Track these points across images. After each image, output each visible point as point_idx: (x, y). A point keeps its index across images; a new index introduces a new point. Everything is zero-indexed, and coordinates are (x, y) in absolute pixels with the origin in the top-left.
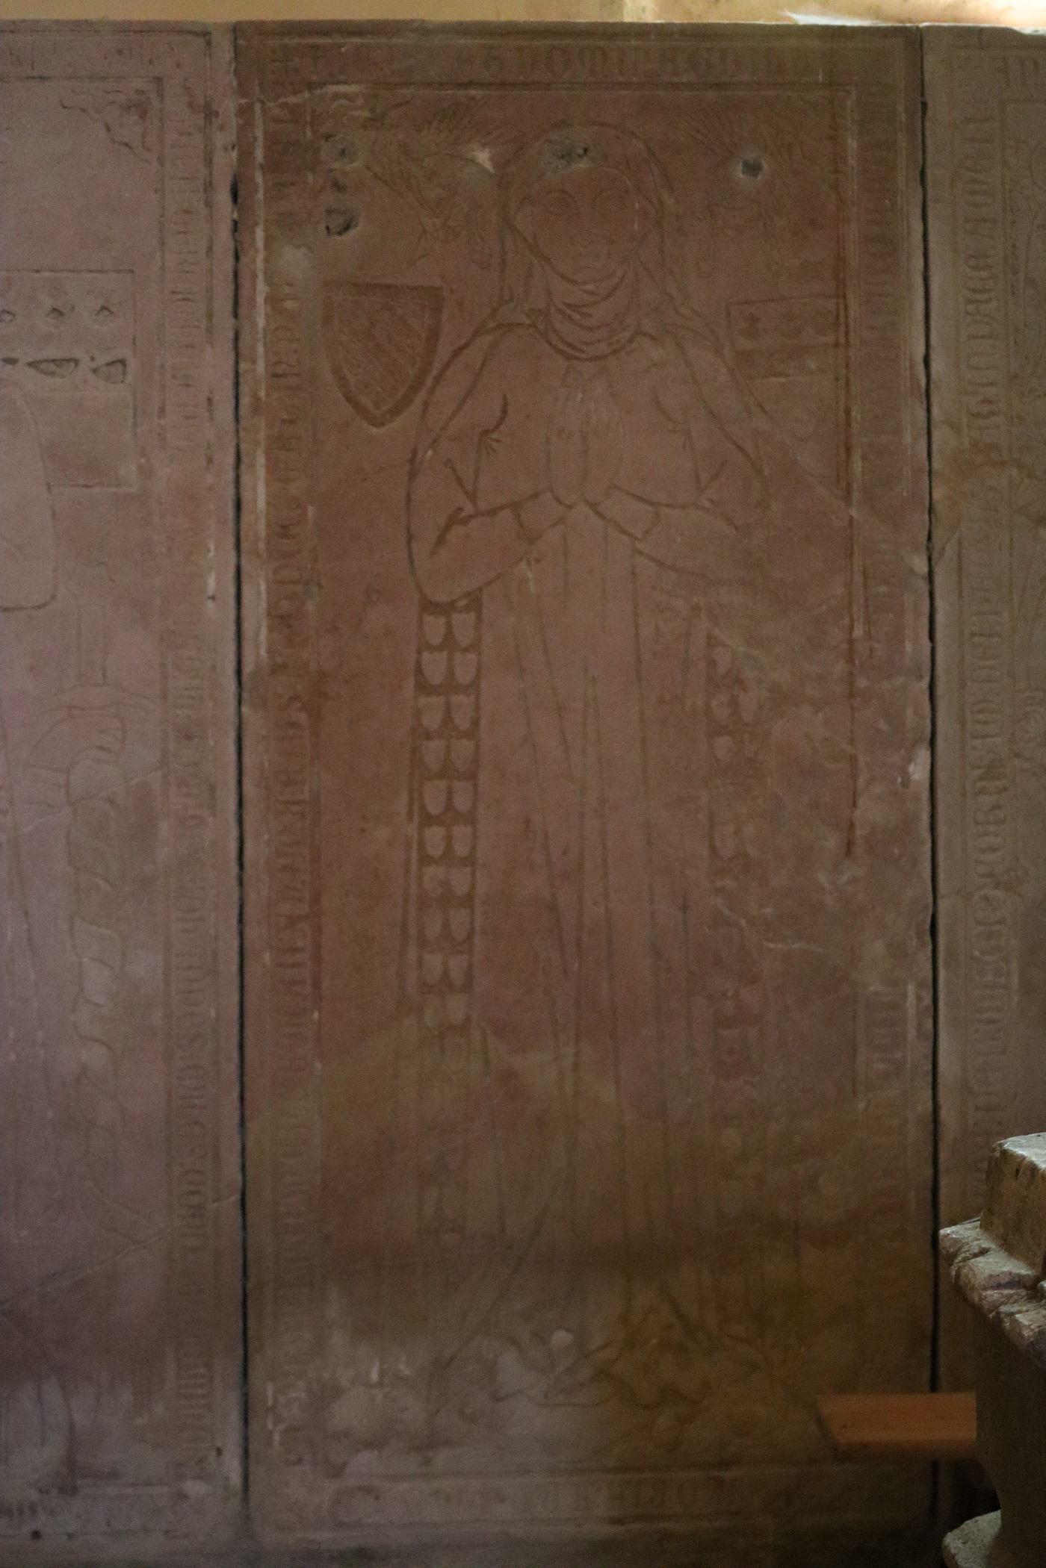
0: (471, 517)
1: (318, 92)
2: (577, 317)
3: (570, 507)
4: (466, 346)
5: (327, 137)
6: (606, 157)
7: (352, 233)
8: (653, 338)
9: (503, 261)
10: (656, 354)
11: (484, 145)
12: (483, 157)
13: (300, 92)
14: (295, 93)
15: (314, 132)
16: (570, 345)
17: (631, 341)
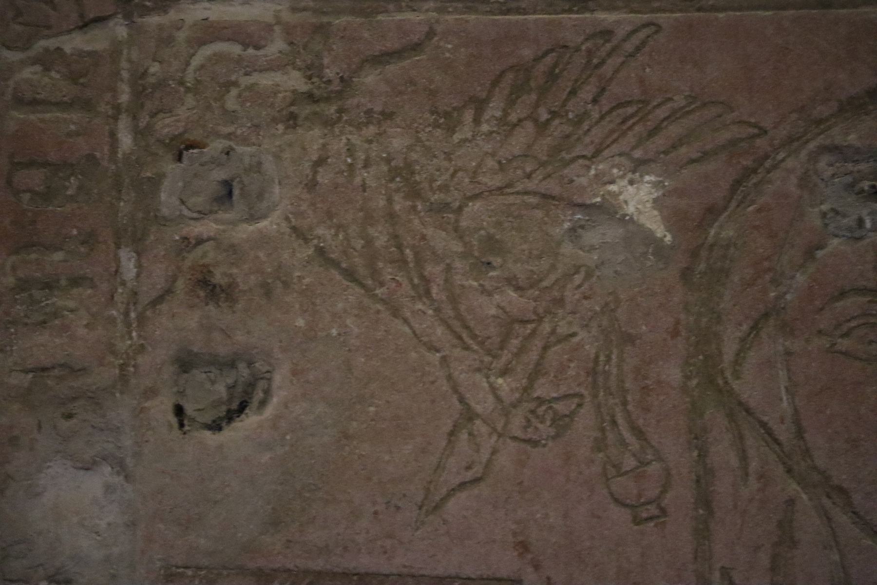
1: (154, 20)
5: (181, 147)
7: (250, 421)
9: (705, 501)
11: (640, 165)
12: (638, 198)
13: (100, 20)
14: (85, 25)
15: (139, 133)
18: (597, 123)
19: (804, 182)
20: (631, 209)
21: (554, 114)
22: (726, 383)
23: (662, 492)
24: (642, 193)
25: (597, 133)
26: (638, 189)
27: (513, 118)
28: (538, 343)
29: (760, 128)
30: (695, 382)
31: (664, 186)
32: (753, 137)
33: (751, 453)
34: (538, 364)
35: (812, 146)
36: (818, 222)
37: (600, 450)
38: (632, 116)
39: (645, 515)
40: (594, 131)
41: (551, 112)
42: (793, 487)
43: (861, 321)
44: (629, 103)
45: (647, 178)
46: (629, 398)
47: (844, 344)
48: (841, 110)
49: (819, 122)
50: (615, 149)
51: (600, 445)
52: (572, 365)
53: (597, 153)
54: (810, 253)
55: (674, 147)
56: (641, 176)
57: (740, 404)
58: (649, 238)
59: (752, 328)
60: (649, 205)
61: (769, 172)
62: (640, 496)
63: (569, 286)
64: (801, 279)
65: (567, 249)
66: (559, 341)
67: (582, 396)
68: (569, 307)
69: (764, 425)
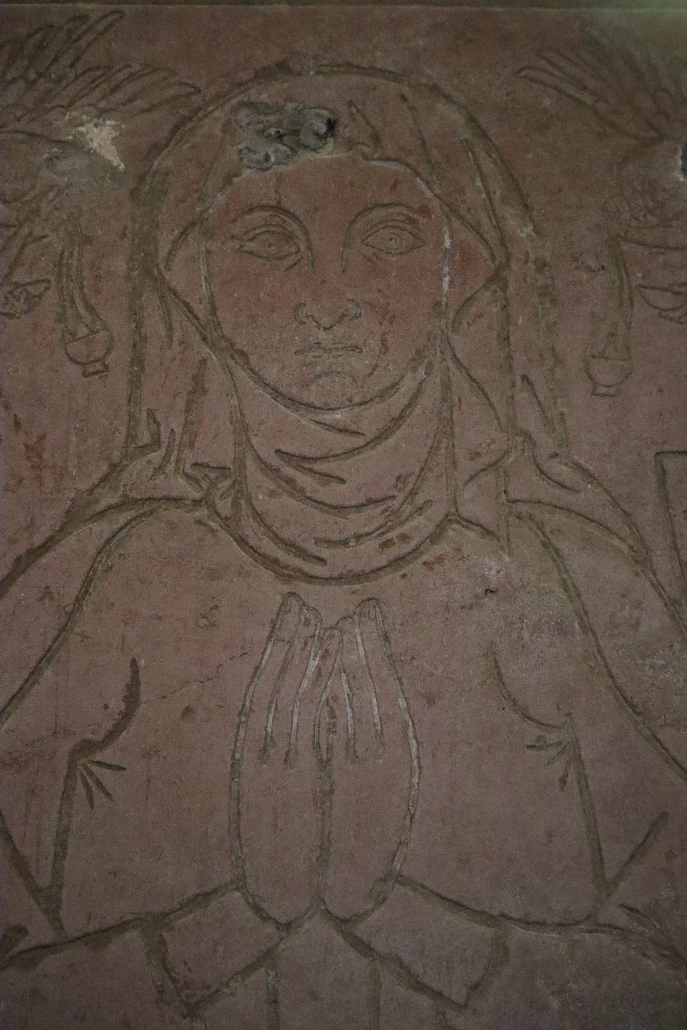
0: (46, 947)
2: (305, 481)
3: (288, 927)
4: (45, 547)
6: (376, 138)
8: (487, 532)
9: (138, 360)
10: (494, 567)
11: (103, 113)
12: (102, 137)
16: (291, 546)
17: (435, 537)
18: (72, 82)
19: (226, 128)
20: (95, 145)
21: (40, 75)
22: (160, 273)
23: (106, 353)
24: (104, 133)
25: (72, 90)
26: (101, 131)
27: (9, 77)
28: (18, 242)
29: (195, 88)
30: (136, 273)
31: (121, 128)
32: (189, 95)
33: (176, 325)
34: (17, 257)
35: (234, 102)
36: (236, 157)
37: (61, 322)
38: (99, 77)
39: (92, 370)
40: (69, 88)
41: (38, 73)
42: (206, 350)
43: (264, 229)
44: (98, 68)
45: (108, 122)
46: (85, 283)
47: (250, 246)
48: (257, 76)
49: (240, 85)
50: (85, 101)
51: (61, 318)
52: (43, 259)
53: (72, 103)
54: (228, 180)
55: (130, 100)
56: (104, 121)
57: (170, 289)
58: (108, 167)
59: (182, 234)
60: (108, 142)
61: (201, 120)
62: (89, 356)
63: (44, 200)
64: (221, 198)
65: (45, 174)
66: (34, 241)
67: (49, 281)
68: (43, 216)
69: (187, 305)
